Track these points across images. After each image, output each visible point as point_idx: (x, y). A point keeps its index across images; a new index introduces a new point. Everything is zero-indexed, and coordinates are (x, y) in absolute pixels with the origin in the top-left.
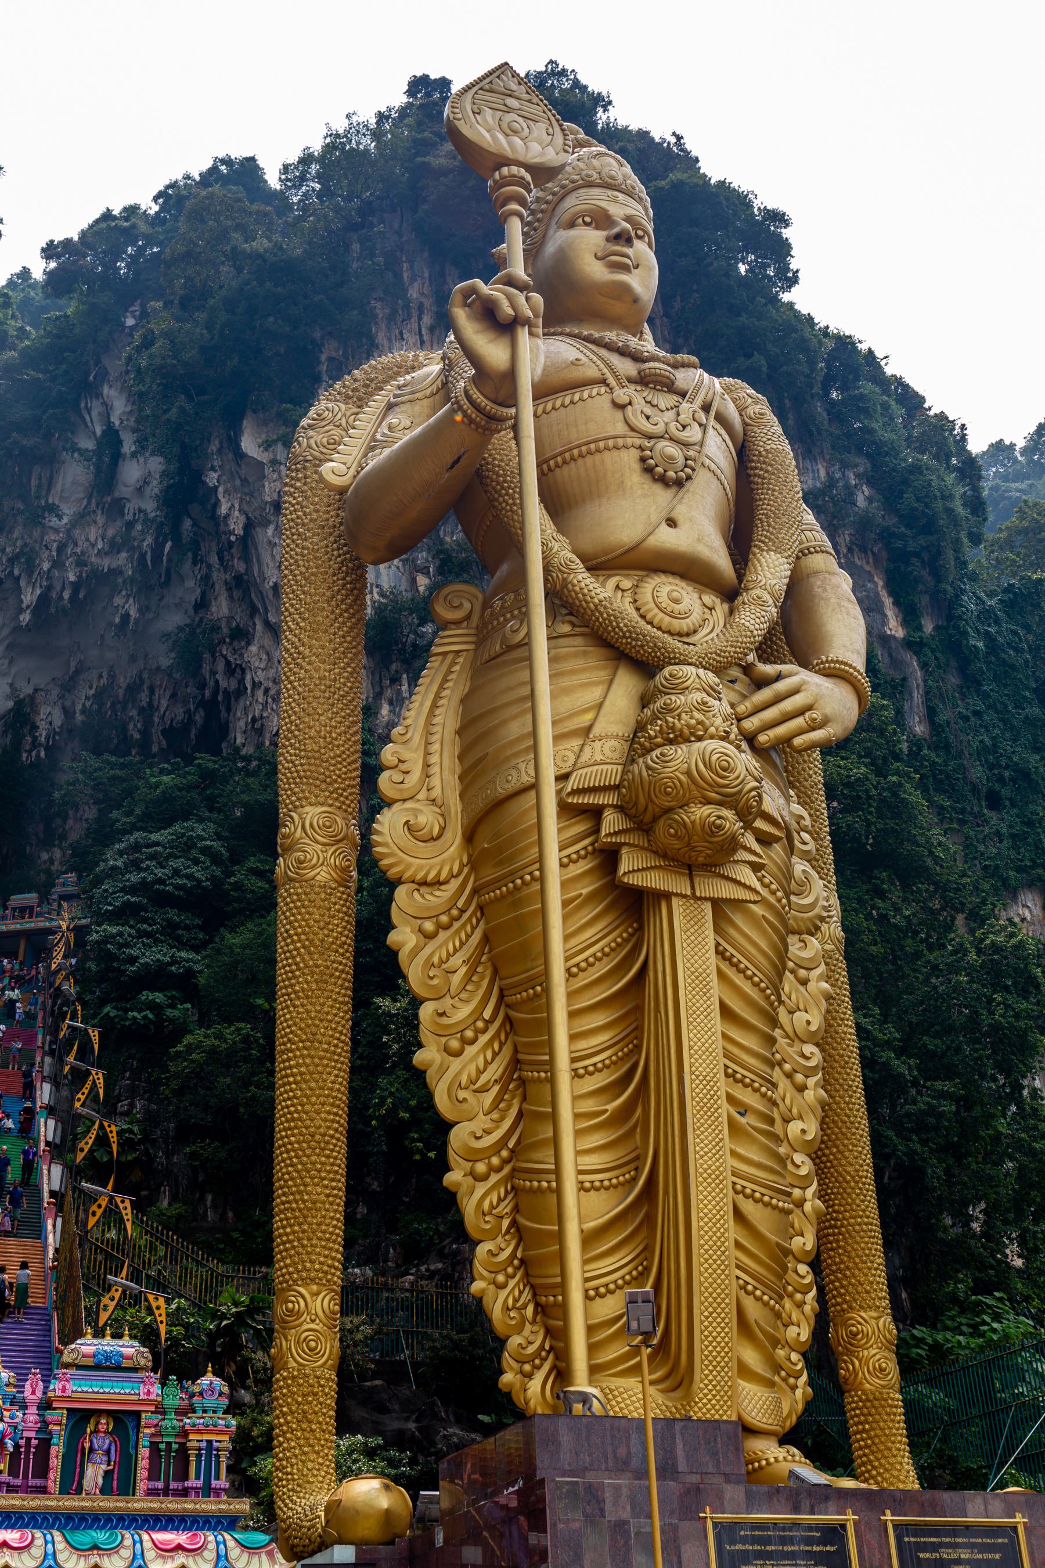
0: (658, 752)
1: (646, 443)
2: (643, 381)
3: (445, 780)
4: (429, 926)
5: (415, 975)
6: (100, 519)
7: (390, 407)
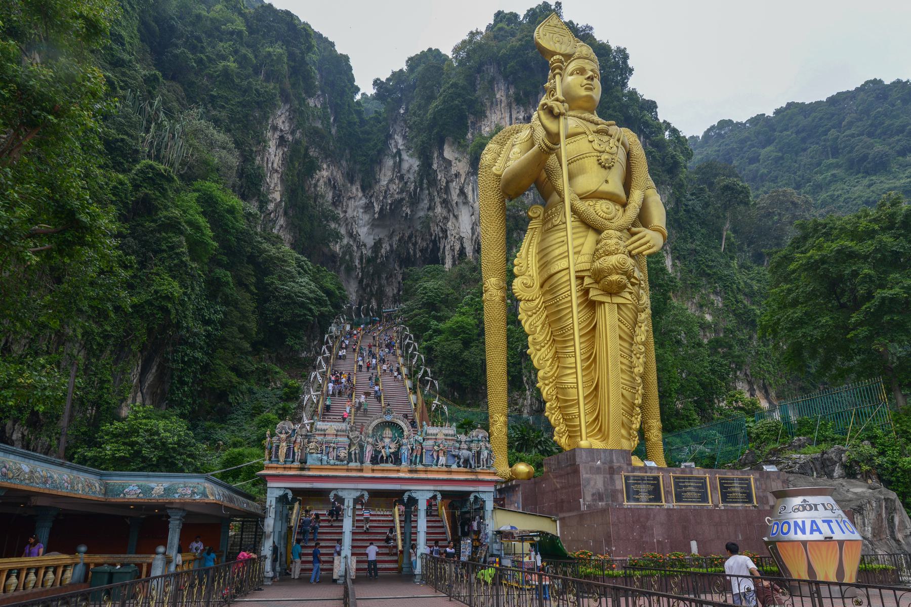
3: (534, 270)
4: (530, 313)
5: (527, 328)
6: (397, 181)
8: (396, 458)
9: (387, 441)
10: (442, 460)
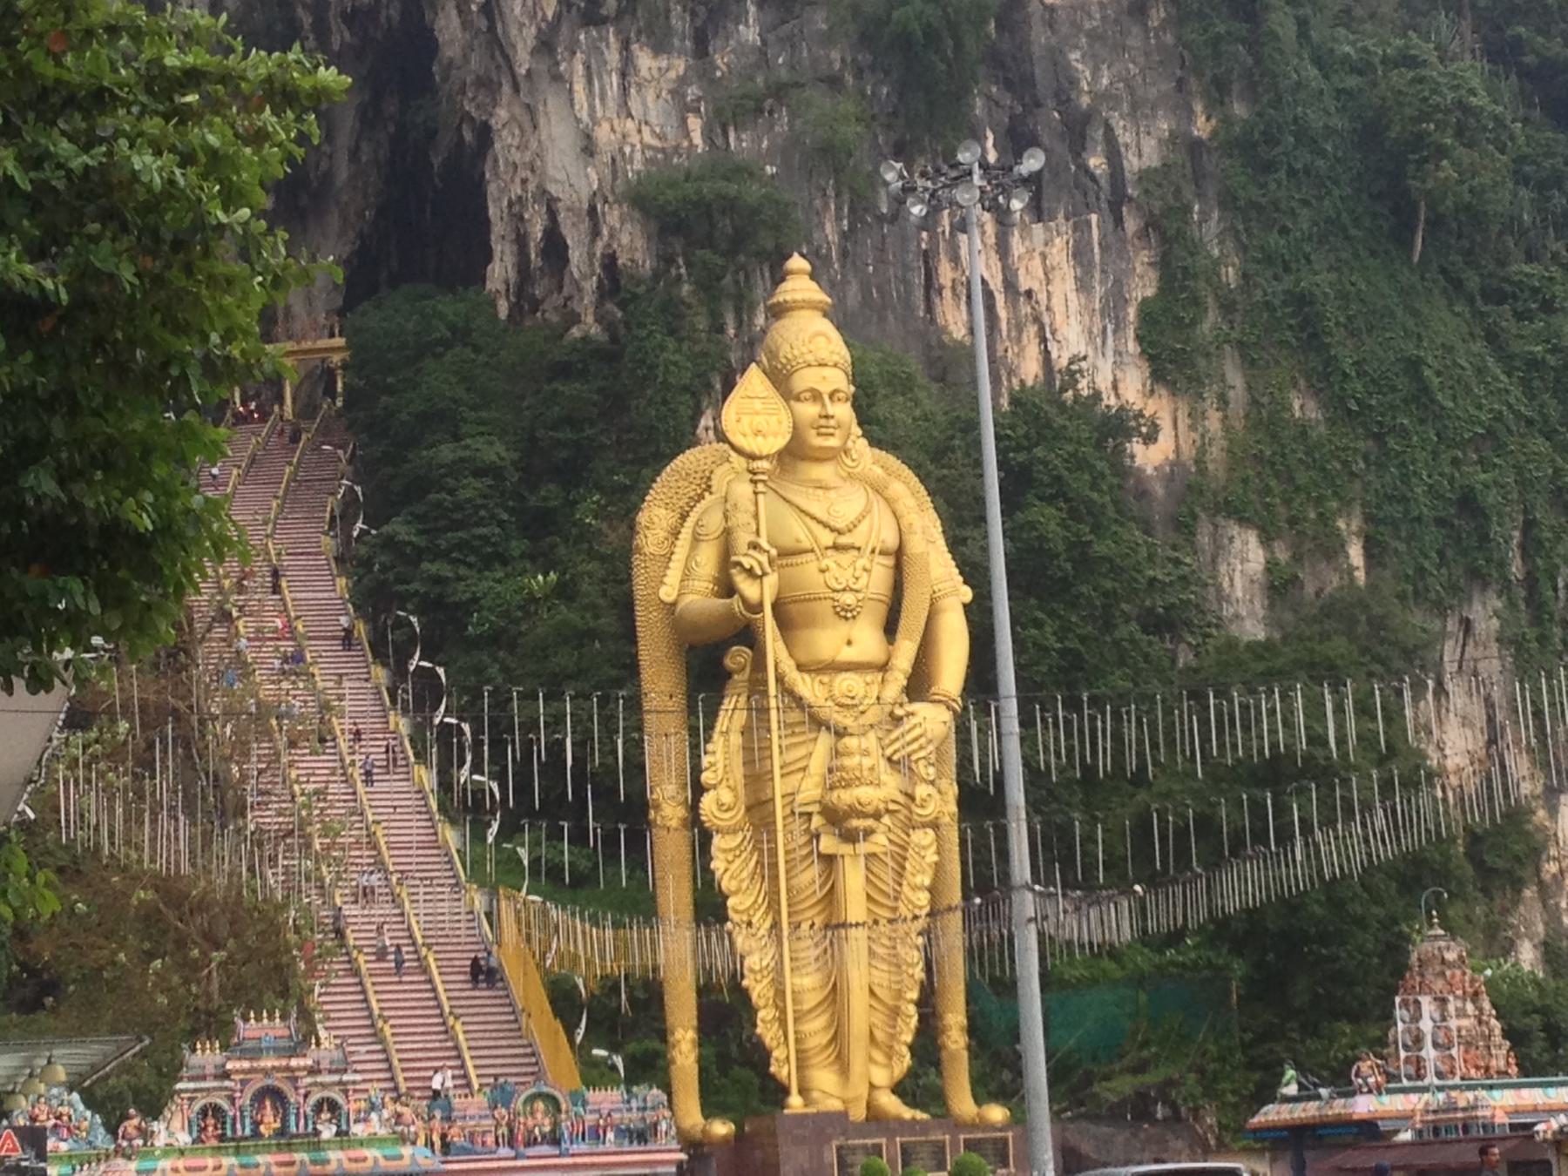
0: (836, 793)
1: (835, 595)
2: (836, 547)
4: (730, 858)
5: (727, 884)
7: (696, 539)
8: (554, 1139)
9: (539, 1116)
10: (610, 1135)
